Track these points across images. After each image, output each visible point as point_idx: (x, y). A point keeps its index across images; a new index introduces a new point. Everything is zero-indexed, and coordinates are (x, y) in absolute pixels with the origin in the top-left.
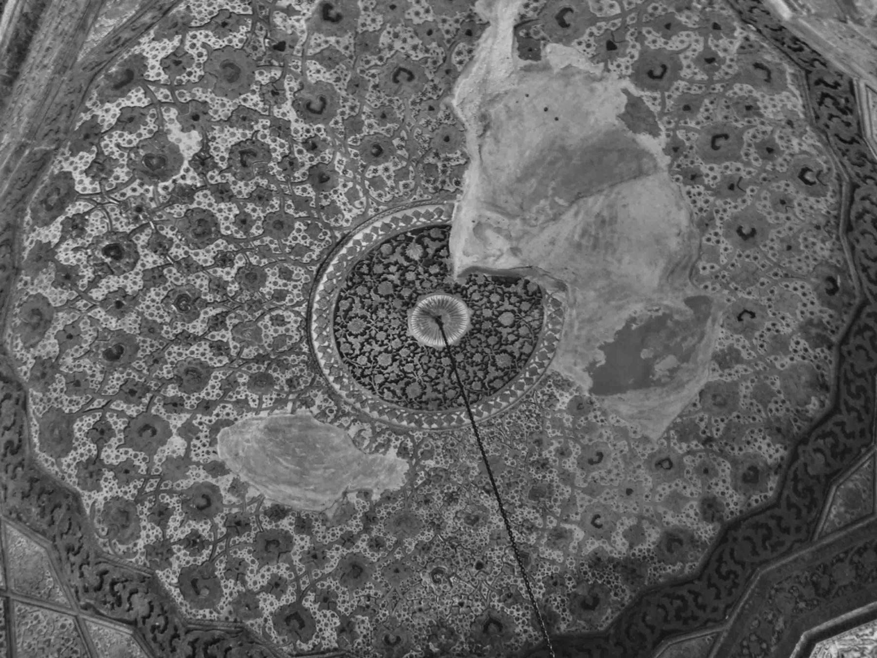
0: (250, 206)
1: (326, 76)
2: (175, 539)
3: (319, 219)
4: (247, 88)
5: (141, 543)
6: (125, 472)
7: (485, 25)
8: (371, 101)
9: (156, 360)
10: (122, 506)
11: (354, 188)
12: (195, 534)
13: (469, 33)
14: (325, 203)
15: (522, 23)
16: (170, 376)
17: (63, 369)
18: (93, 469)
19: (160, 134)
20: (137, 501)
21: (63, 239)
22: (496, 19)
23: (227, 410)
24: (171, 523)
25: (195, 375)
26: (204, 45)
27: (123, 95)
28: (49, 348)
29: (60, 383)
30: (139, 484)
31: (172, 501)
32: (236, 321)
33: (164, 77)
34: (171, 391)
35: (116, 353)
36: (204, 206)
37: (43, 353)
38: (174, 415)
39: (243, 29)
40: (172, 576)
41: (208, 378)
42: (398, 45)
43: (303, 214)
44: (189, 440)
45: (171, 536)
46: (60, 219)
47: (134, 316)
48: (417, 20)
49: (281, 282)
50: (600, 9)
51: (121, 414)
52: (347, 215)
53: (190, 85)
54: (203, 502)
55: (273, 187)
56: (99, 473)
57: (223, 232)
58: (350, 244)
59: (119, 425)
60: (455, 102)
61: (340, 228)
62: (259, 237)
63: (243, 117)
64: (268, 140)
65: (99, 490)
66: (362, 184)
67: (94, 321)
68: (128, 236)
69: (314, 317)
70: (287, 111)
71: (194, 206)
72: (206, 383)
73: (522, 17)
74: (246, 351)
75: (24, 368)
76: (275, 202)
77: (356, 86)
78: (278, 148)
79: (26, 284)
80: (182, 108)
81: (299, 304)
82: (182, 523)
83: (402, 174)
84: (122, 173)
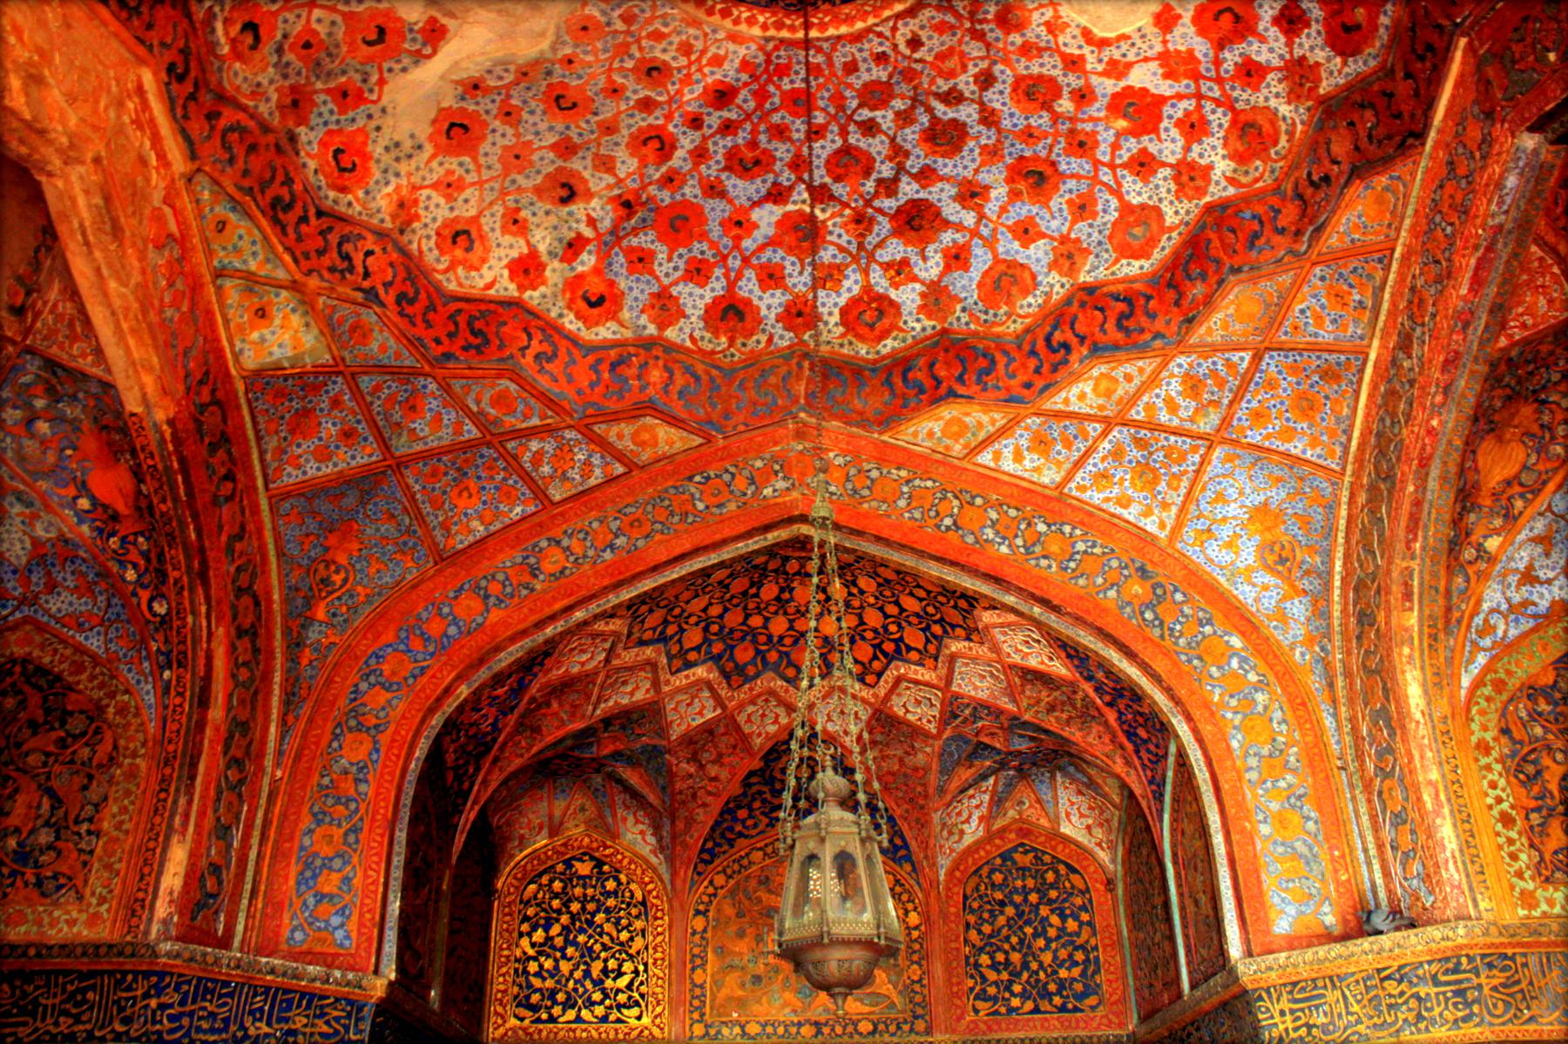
0: (796, 136)
1: (621, 154)
2: (1284, 51)
3: (766, 71)
4: (686, 203)
5: (1285, 109)
6: (1194, 128)
7: (457, 82)
8: (608, 110)
9: (1029, 135)
10: (1236, 133)
11: (709, 64)
12: (1276, 21)
13: (476, 87)
14: (745, 77)
15: (419, 57)
16: (1045, 114)
17: (1065, 230)
18: (1190, 176)
19: (772, 242)
20: (1232, 109)
21: (915, 279)
22: (442, 77)
23: (1069, 40)
24: (1262, 59)
25: (1037, 92)
26: (670, 260)
27: (748, 302)
28: (1040, 254)
29: (1082, 230)
30: (1208, 106)
31: (1231, 58)
32: (940, 82)
33: (718, 272)
34: (1065, 105)
35: (1035, 178)
36: (823, 171)
37: (1045, 261)
38: (1099, 91)
39: (635, 241)
40: (1331, 66)
41: (1030, 77)
42: (543, 126)
43: (771, 88)
44: (1129, 65)
45: (1281, 57)
46: (893, 294)
47: (980, 177)
48: (510, 131)
49: (863, 67)
50: (333, 23)
51: (1115, 146)
52: (742, 51)
53: (713, 245)
54: (1226, 19)
55: (762, 128)
56: (1192, 166)
57: (839, 143)
58: (772, 32)
59: (1131, 146)
60: (545, 45)
61: (761, 48)
62: (823, 110)
63: (714, 190)
64: (720, 157)
65: (1210, 167)
66: (699, 59)
67: (1003, 210)
68: (893, 218)
69: (887, 13)
70: (679, 159)
71: (828, 180)
72: (1041, 77)
73: (416, 63)
74: (975, 54)
75: (1057, 288)
76: (776, 118)
77: (609, 129)
78: (720, 147)
79: (964, 310)
80: (738, 239)
81: (880, 35)
82: (1263, 40)
83: (657, 36)
84: (827, 255)
